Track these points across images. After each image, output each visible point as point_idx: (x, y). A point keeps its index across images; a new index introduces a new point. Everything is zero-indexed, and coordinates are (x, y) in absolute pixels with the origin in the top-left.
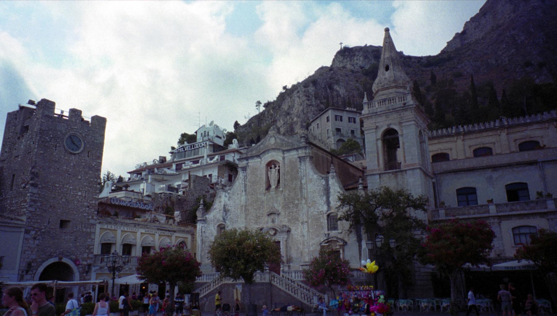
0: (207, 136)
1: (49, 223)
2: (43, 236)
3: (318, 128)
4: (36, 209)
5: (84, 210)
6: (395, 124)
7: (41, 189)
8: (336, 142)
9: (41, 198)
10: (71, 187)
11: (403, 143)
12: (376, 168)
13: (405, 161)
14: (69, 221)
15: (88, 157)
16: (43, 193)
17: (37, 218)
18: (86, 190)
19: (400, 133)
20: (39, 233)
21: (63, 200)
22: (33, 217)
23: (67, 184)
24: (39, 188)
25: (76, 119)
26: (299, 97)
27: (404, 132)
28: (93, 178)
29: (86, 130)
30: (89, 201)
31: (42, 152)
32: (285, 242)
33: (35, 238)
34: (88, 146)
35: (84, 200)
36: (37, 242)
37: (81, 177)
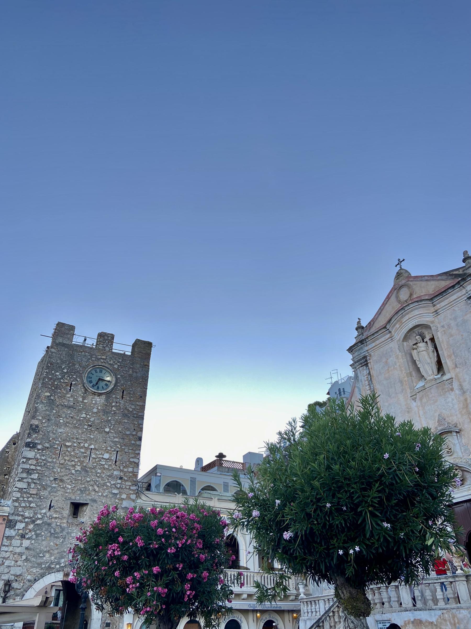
0: (342, 393)
1: (50, 509)
2: (38, 532)
4: (29, 484)
5: (114, 484)
7: (41, 451)
9: (40, 466)
10: (92, 447)
14: (87, 504)
15: (122, 397)
16: (43, 458)
17: (30, 499)
18: (118, 450)
20: (31, 527)
21: (78, 468)
22: (24, 498)
23: (86, 441)
24: (39, 450)
25: (105, 346)
28: (129, 430)
29: (121, 360)
30: (121, 468)
31: (48, 394)
33: (23, 536)
34: (122, 382)
35: (114, 466)
36: (26, 543)
37: (110, 429)
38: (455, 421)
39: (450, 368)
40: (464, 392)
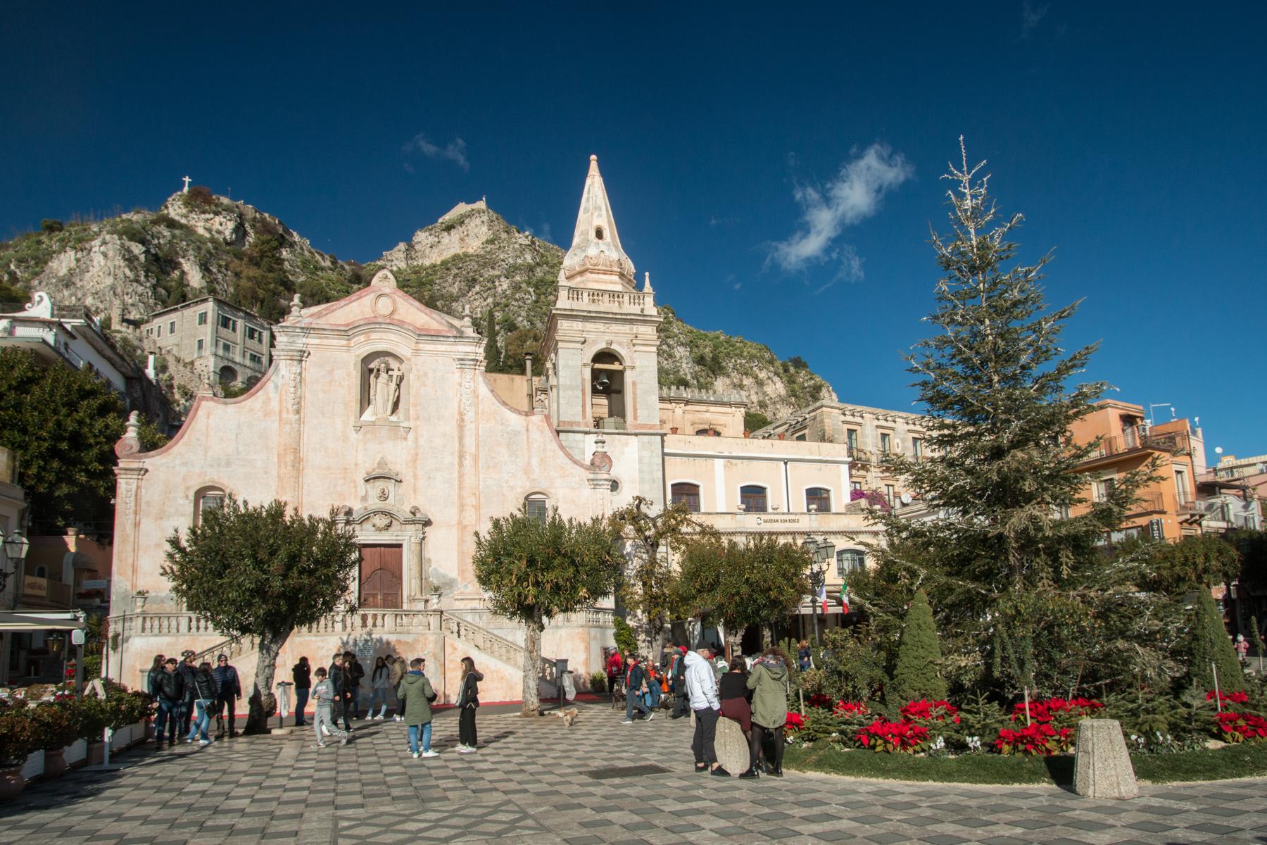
3: (172, 331)
6: (620, 344)
8: (218, 371)
11: (634, 384)
12: (579, 419)
13: (635, 418)
19: (627, 363)
26: (105, 255)
27: (638, 364)
32: (416, 548)
38: (397, 470)
39: (411, 417)
40: (417, 447)
